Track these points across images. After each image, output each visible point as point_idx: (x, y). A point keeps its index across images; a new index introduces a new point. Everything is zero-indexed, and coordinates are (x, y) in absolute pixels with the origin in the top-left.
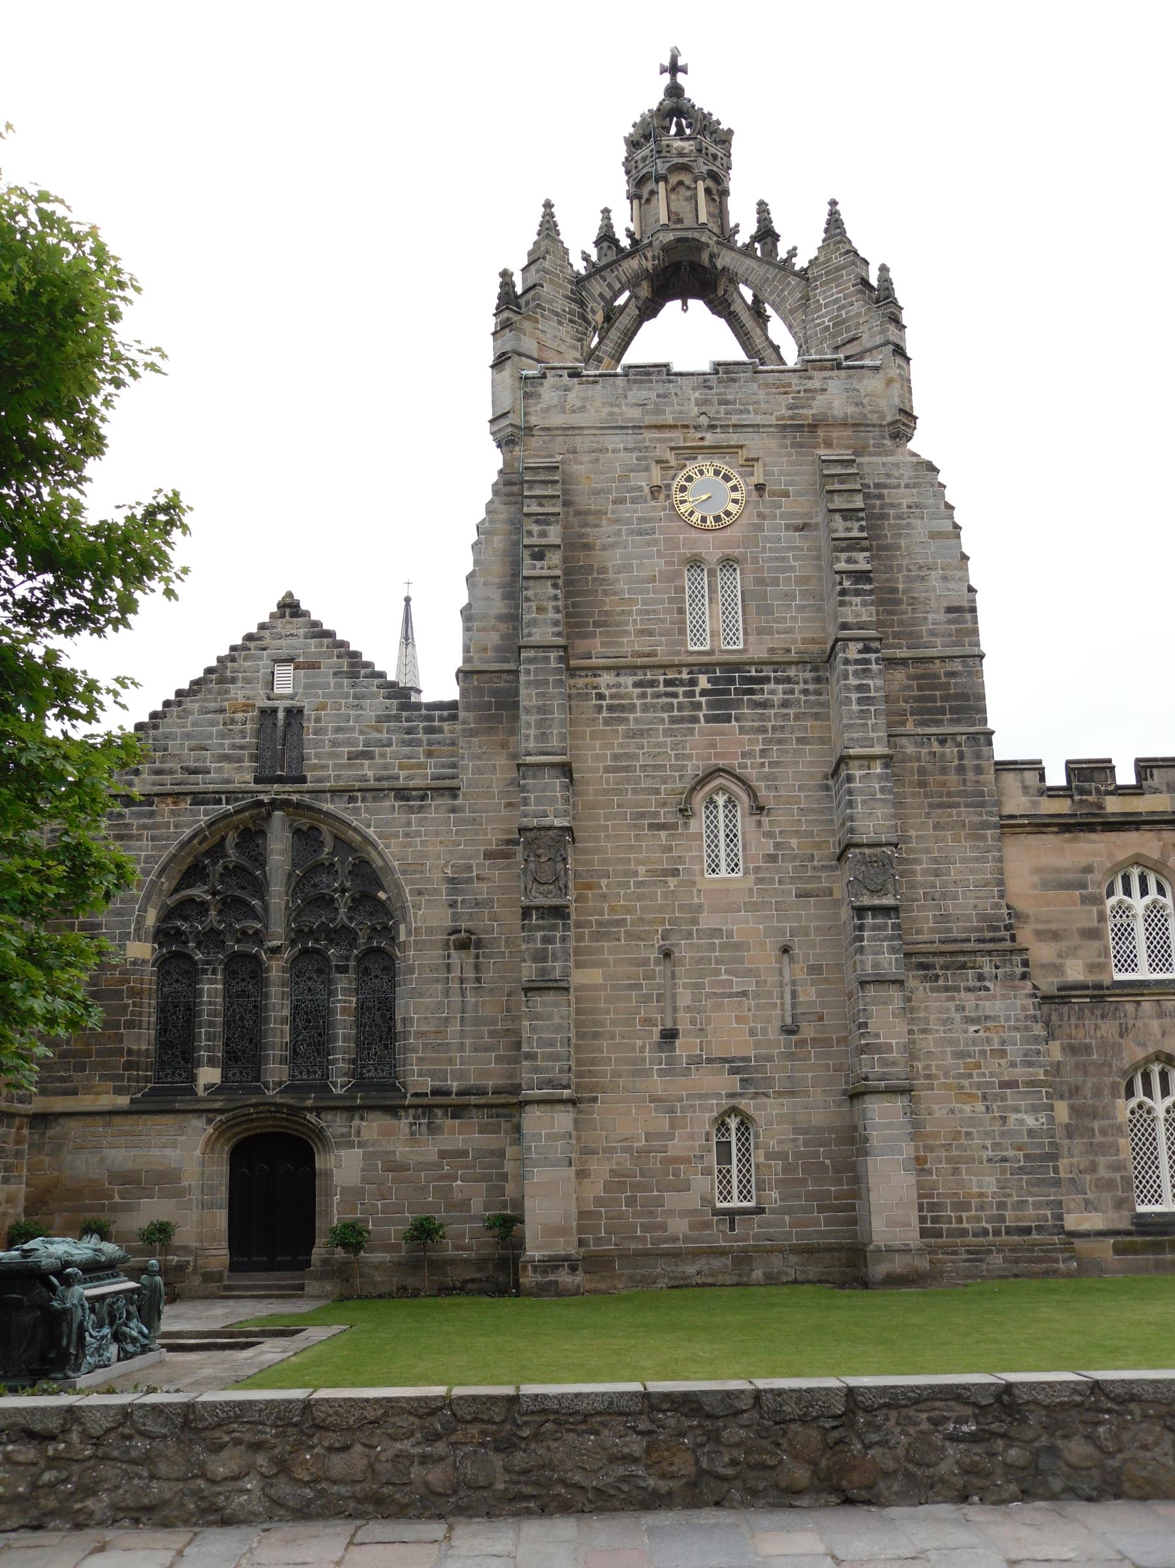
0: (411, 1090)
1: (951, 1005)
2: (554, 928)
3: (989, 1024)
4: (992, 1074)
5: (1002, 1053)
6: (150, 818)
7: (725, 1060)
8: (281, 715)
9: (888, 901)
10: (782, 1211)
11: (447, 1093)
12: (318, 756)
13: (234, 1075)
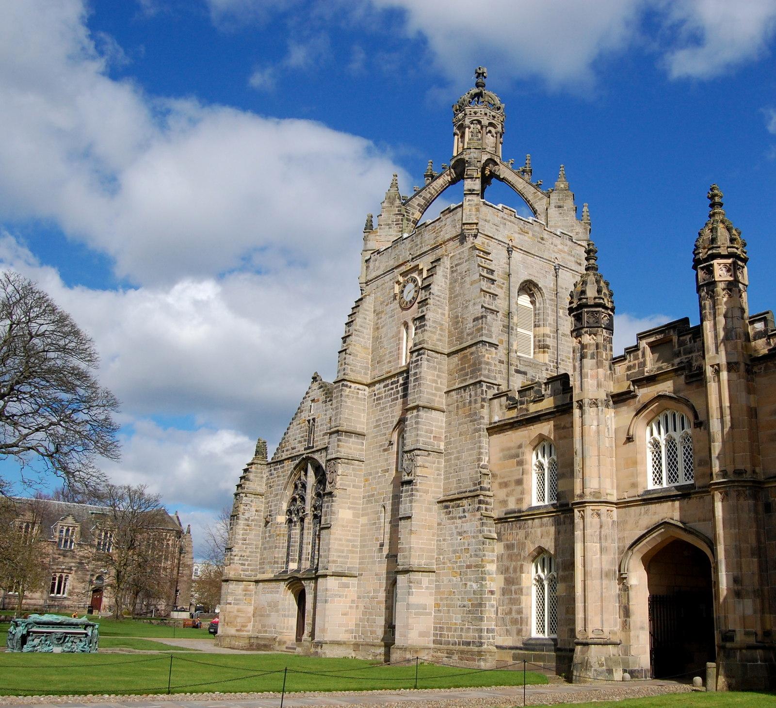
1: (453, 526)
3: (465, 535)
4: (464, 562)
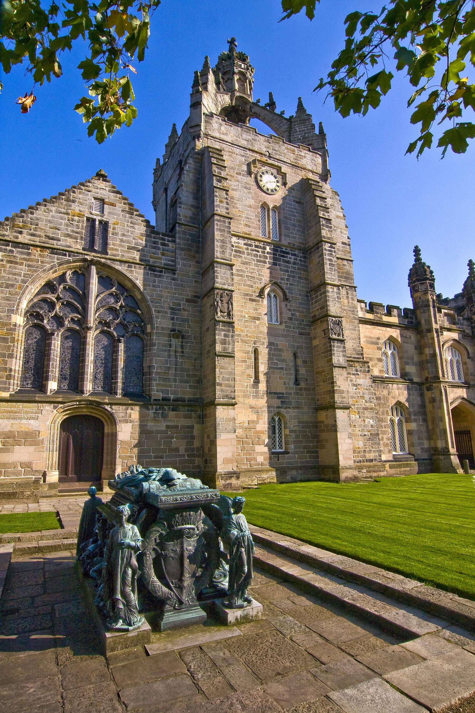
0: (153, 398)
2: (229, 331)
3: (359, 387)
5: (363, 397)
6: (28, 255)
7: (275, 393)
8: (97, 223)
9: (341, 338)
10: (295, 453)
11: (168, 400)
12: (114, 244)
13: (64, 386)
